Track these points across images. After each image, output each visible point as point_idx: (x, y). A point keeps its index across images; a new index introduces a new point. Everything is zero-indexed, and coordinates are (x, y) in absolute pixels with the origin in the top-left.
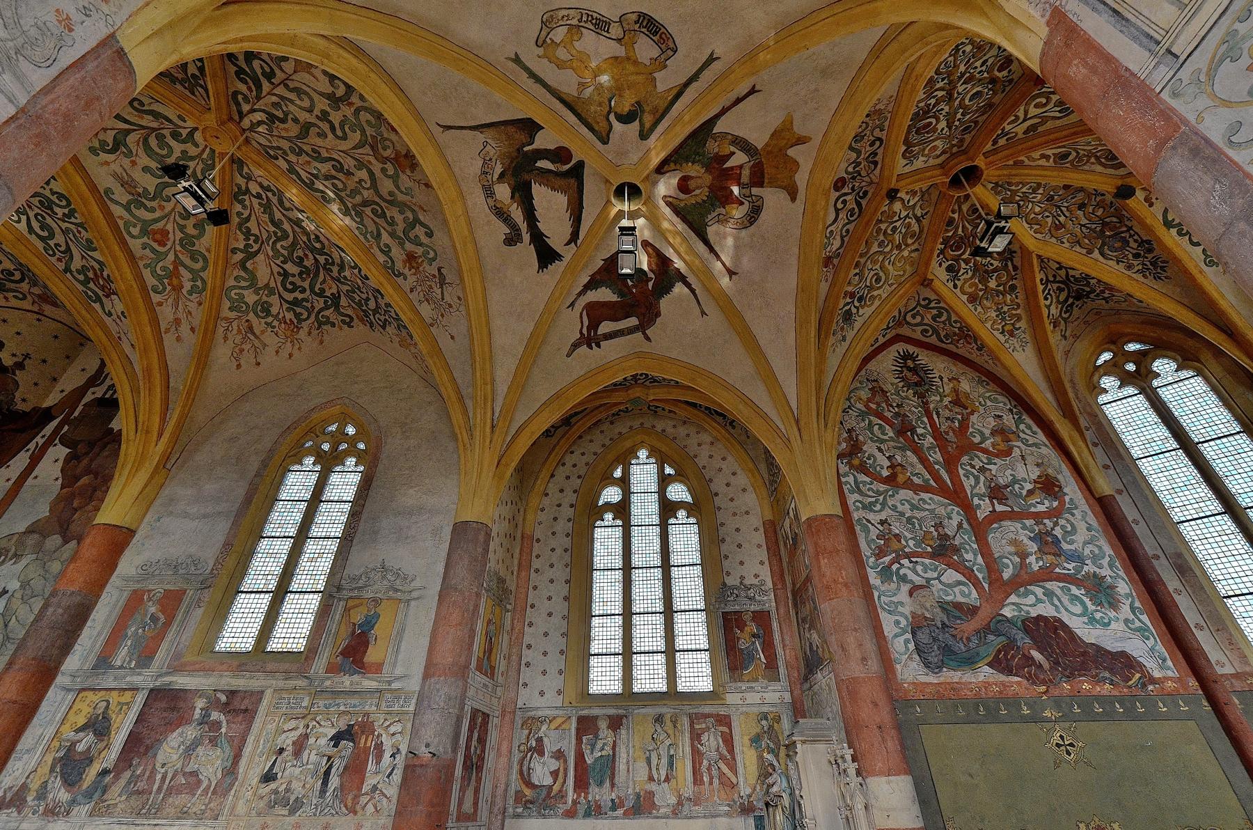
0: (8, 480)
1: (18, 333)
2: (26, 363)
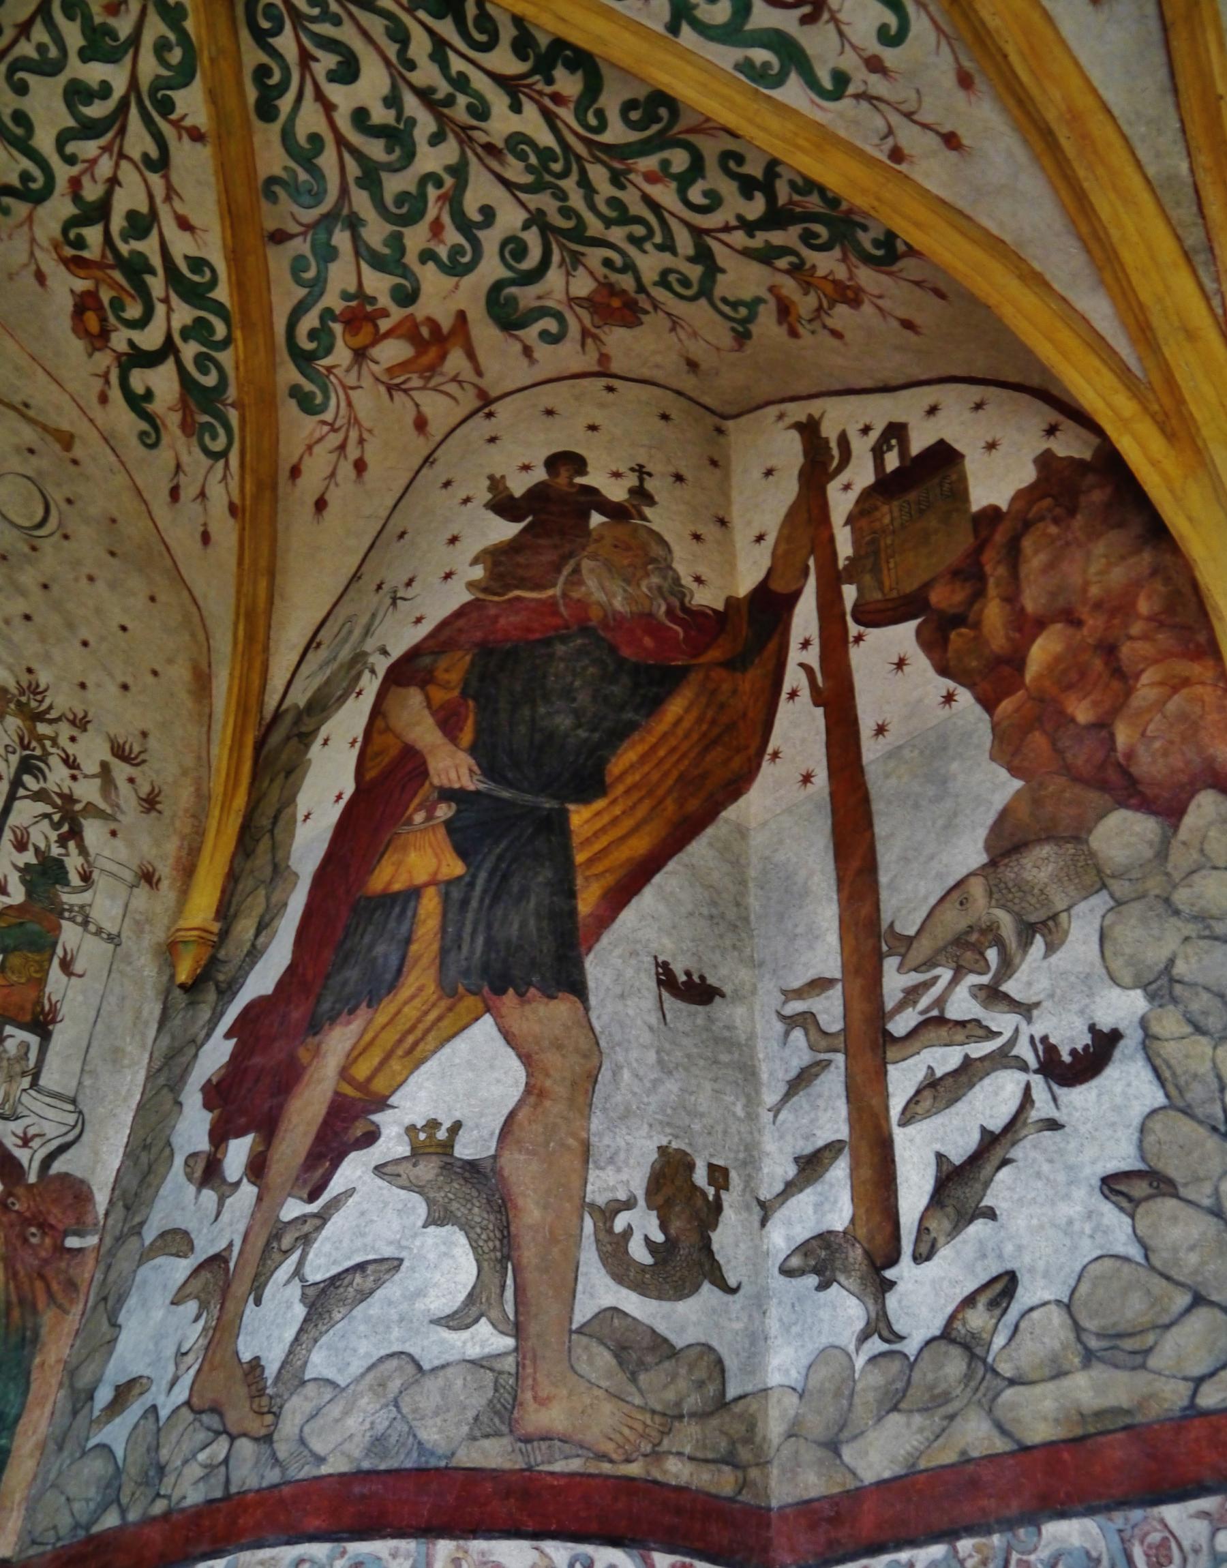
0: (807, 779)
1: (593, 428)
2: (650, 485)
